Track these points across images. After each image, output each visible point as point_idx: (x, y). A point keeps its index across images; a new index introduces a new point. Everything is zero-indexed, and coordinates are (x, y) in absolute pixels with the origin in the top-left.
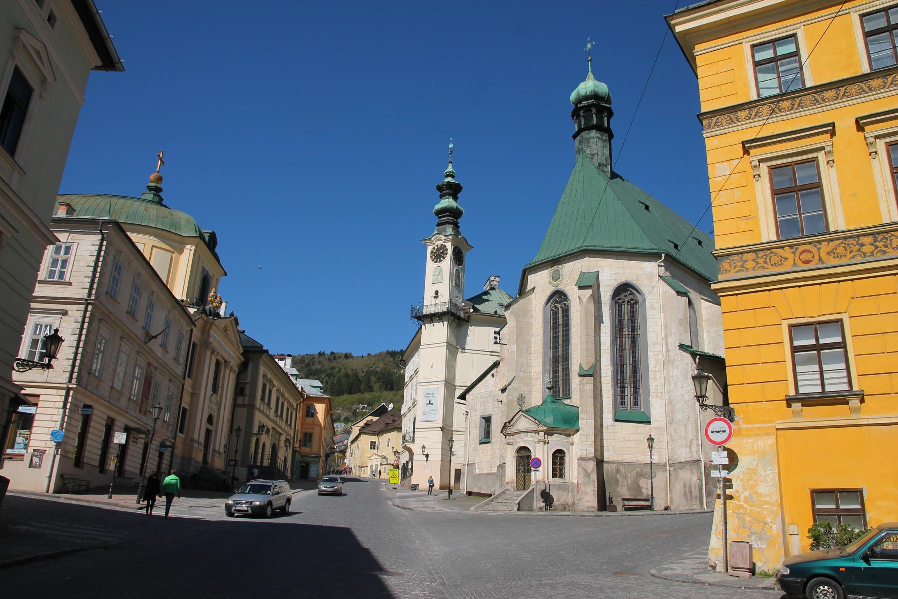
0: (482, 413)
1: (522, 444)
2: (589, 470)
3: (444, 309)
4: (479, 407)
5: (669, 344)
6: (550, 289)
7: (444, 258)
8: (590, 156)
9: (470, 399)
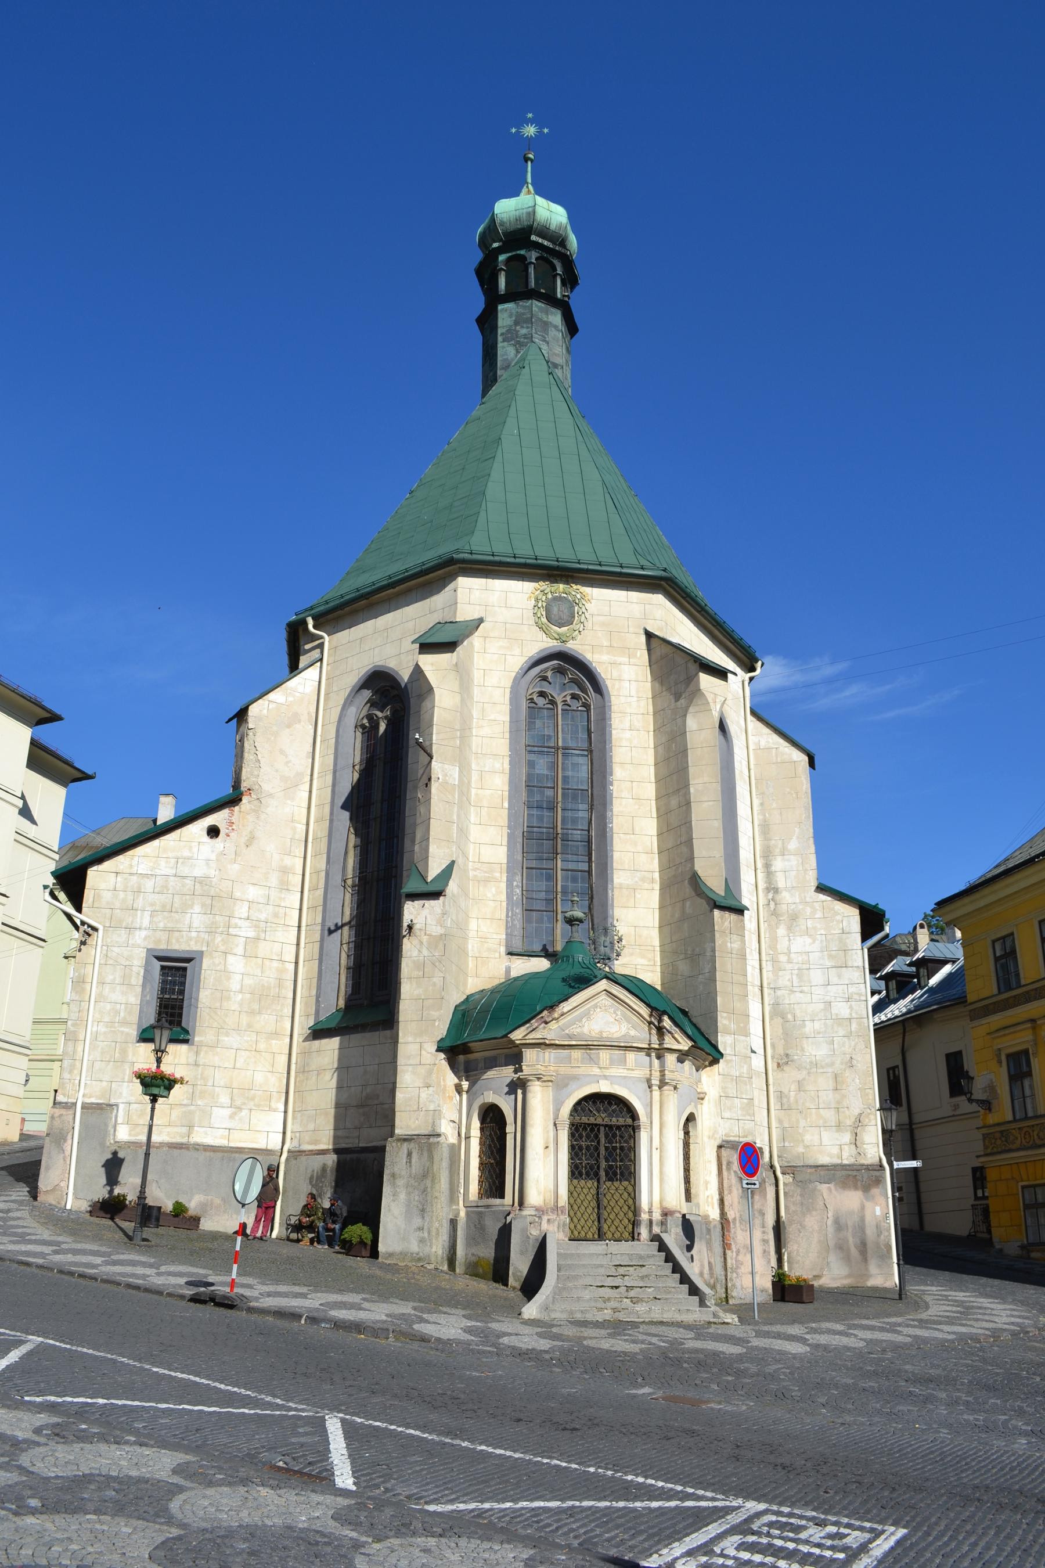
1: (605, 1087)
6: (540, 643)
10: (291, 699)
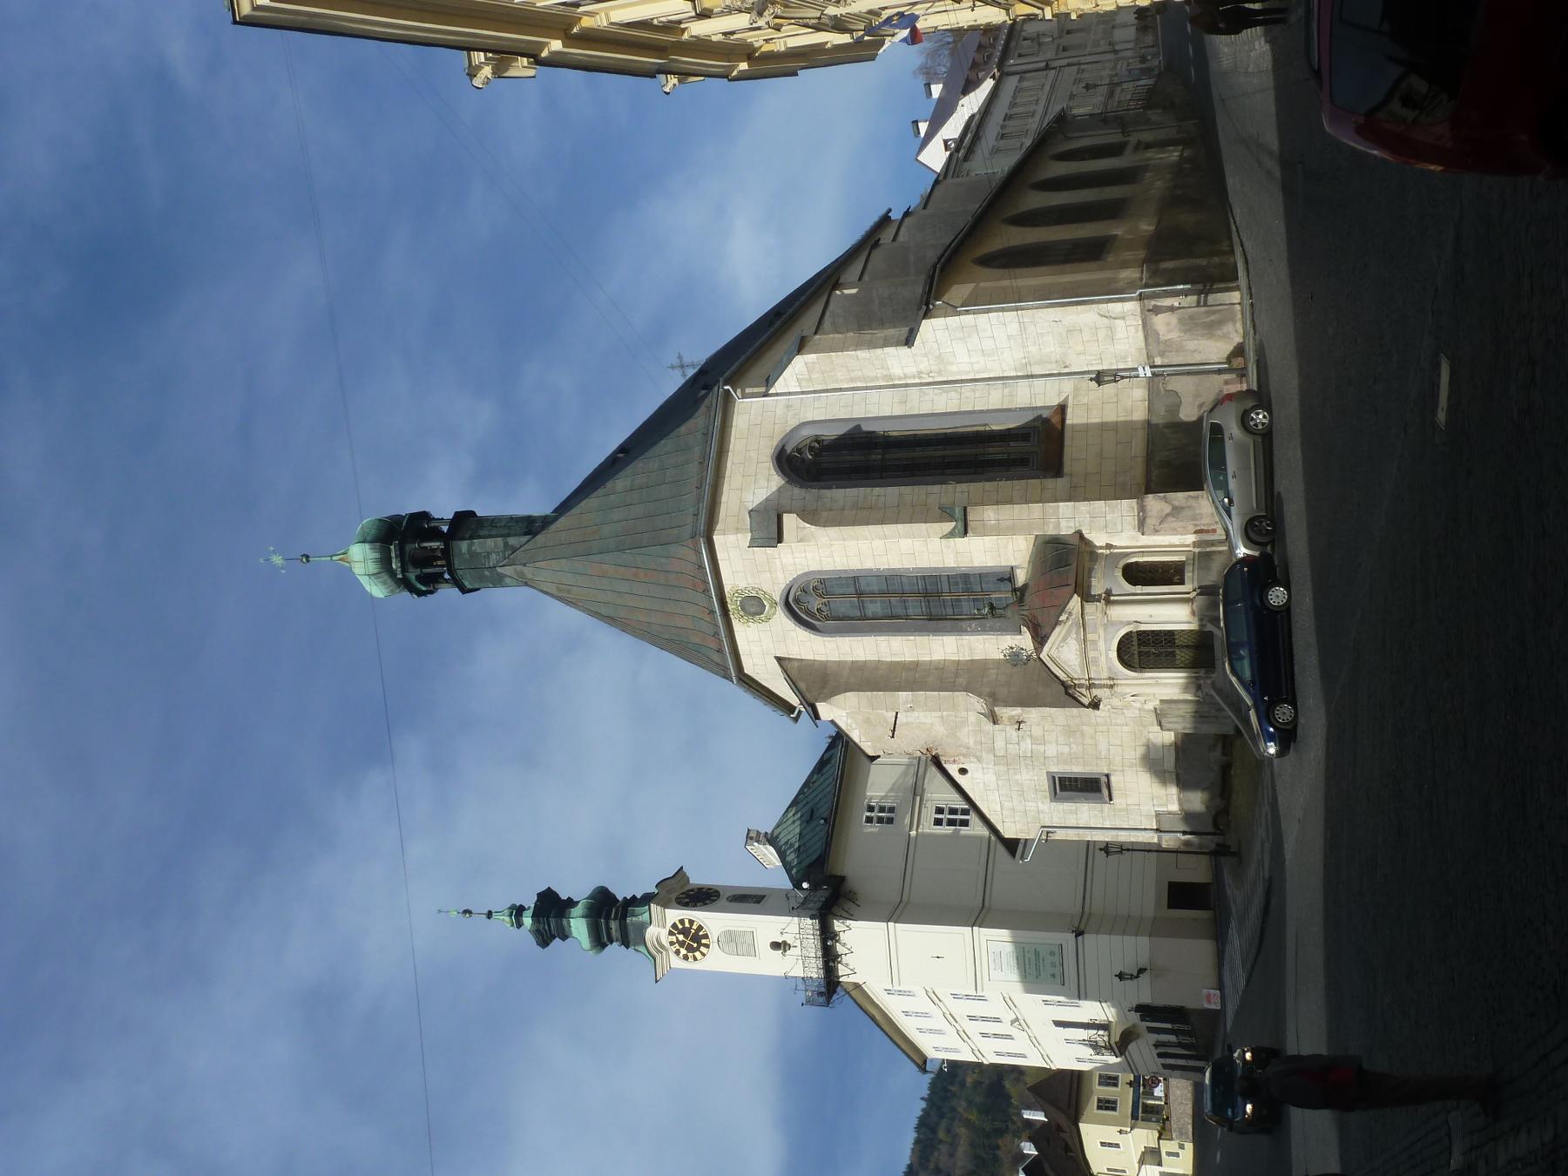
0: (1045, 797)
1: (1114, 654)
2: (1167, 509)
3: (810, 924)
4: (1031, 806)
5: (906, 370)
7: (700, 928)
9: (1013, 829)
10: (854, 726)
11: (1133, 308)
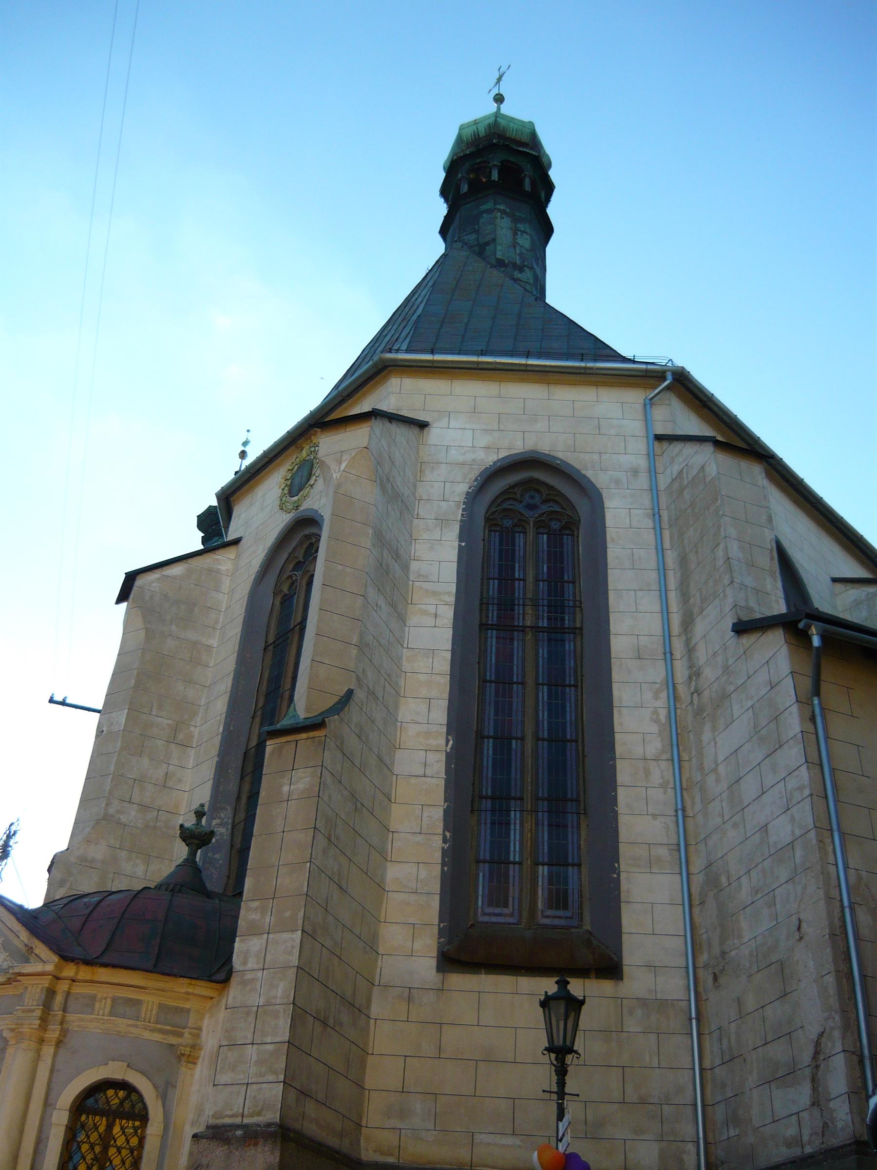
8: (477, 249)
11: (840, 1125)
